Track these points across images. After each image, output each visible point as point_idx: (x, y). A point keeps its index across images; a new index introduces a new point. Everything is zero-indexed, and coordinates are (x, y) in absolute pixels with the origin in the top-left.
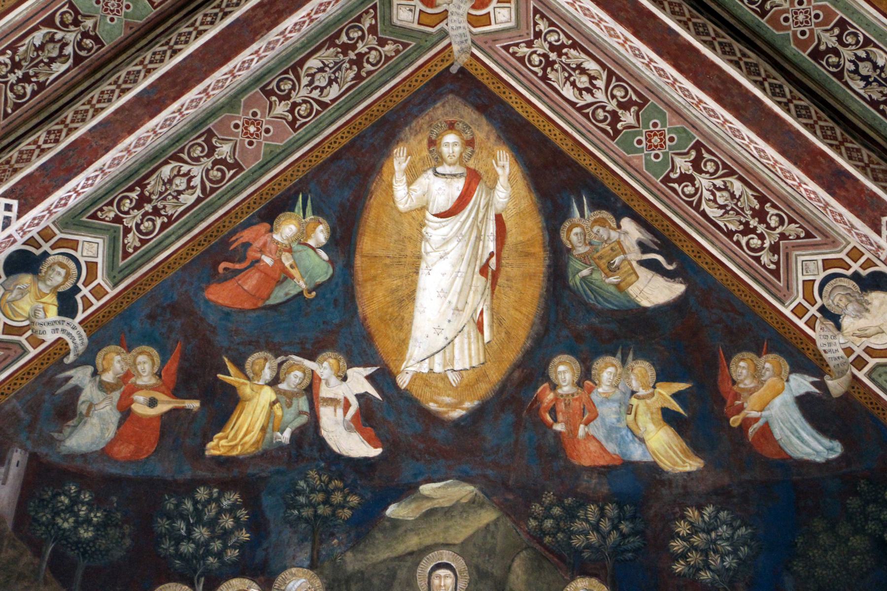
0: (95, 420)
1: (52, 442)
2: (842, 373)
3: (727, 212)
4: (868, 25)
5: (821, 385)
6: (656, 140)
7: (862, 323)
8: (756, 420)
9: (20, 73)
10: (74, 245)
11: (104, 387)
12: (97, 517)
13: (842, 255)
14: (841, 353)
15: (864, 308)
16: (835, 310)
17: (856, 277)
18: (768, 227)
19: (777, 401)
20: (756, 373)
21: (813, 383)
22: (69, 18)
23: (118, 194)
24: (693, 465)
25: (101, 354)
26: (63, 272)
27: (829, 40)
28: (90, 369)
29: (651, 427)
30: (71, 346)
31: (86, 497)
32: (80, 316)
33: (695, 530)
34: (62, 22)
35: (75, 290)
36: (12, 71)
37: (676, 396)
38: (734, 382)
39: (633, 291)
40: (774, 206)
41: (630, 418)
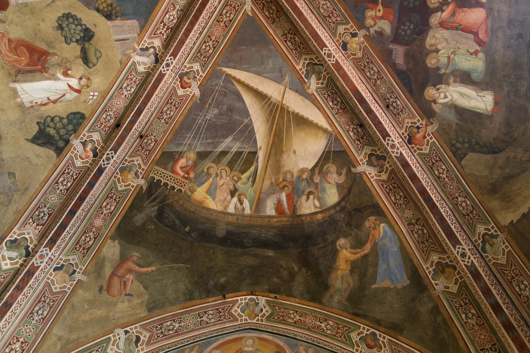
0: (383, 26)
1: (388, 37)
9: (298, 48)
10: (340, 34)
11: (375, 25)
12: (408, 24)
22: (285, 36)
23: (328, 23)
25: (367, 26)
26: (347, 36)
28: (370, 28)
30: (364, 33)
31: (402, 27)
32: (357, 32)
34: (286, 38)
35: (351, 33)
36: (297, 50)
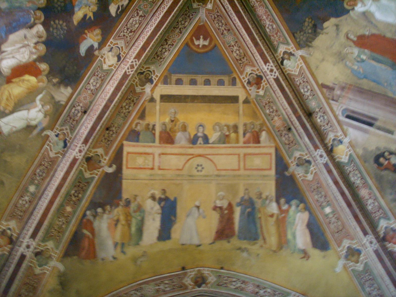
2: (99, 54)
3: (131, 24)
4: (173, 50)
5: (96, 49)
6: (146, 6)
7: (110, 56)
8: (87, 36)
13: (124, 50)
14: (103, 53)
15: (113, 56)
16: (113, 50)
17: (120, 54)
18: (129, 33)
19: (92, 40)
20: (97, 35)
21: (96, 48)
24: (75, 23)
27: (169, 43)
29: (83, 12)
33: (61, 25)
37: (90, 17)
38: (94, 30)
39: (113, 4)
40: (133, 34)
41: (84, 6)
